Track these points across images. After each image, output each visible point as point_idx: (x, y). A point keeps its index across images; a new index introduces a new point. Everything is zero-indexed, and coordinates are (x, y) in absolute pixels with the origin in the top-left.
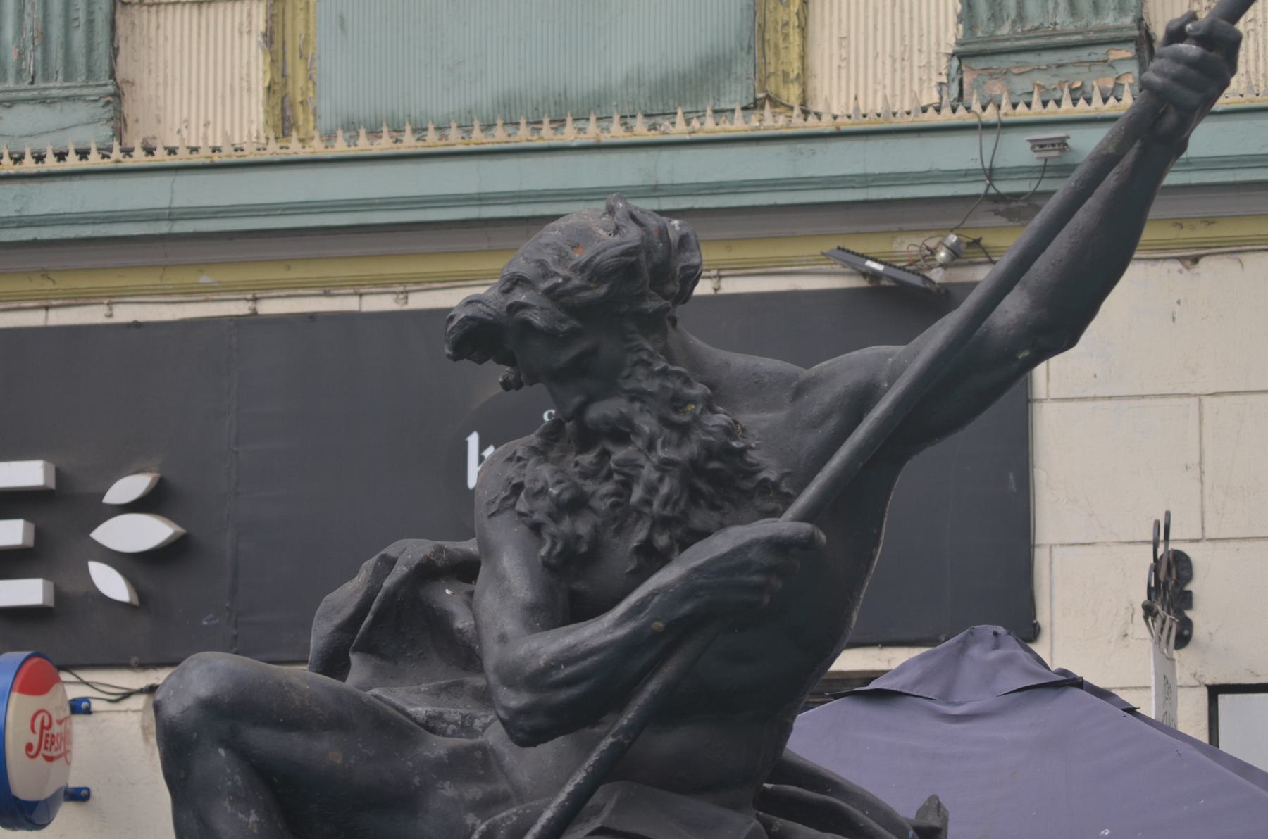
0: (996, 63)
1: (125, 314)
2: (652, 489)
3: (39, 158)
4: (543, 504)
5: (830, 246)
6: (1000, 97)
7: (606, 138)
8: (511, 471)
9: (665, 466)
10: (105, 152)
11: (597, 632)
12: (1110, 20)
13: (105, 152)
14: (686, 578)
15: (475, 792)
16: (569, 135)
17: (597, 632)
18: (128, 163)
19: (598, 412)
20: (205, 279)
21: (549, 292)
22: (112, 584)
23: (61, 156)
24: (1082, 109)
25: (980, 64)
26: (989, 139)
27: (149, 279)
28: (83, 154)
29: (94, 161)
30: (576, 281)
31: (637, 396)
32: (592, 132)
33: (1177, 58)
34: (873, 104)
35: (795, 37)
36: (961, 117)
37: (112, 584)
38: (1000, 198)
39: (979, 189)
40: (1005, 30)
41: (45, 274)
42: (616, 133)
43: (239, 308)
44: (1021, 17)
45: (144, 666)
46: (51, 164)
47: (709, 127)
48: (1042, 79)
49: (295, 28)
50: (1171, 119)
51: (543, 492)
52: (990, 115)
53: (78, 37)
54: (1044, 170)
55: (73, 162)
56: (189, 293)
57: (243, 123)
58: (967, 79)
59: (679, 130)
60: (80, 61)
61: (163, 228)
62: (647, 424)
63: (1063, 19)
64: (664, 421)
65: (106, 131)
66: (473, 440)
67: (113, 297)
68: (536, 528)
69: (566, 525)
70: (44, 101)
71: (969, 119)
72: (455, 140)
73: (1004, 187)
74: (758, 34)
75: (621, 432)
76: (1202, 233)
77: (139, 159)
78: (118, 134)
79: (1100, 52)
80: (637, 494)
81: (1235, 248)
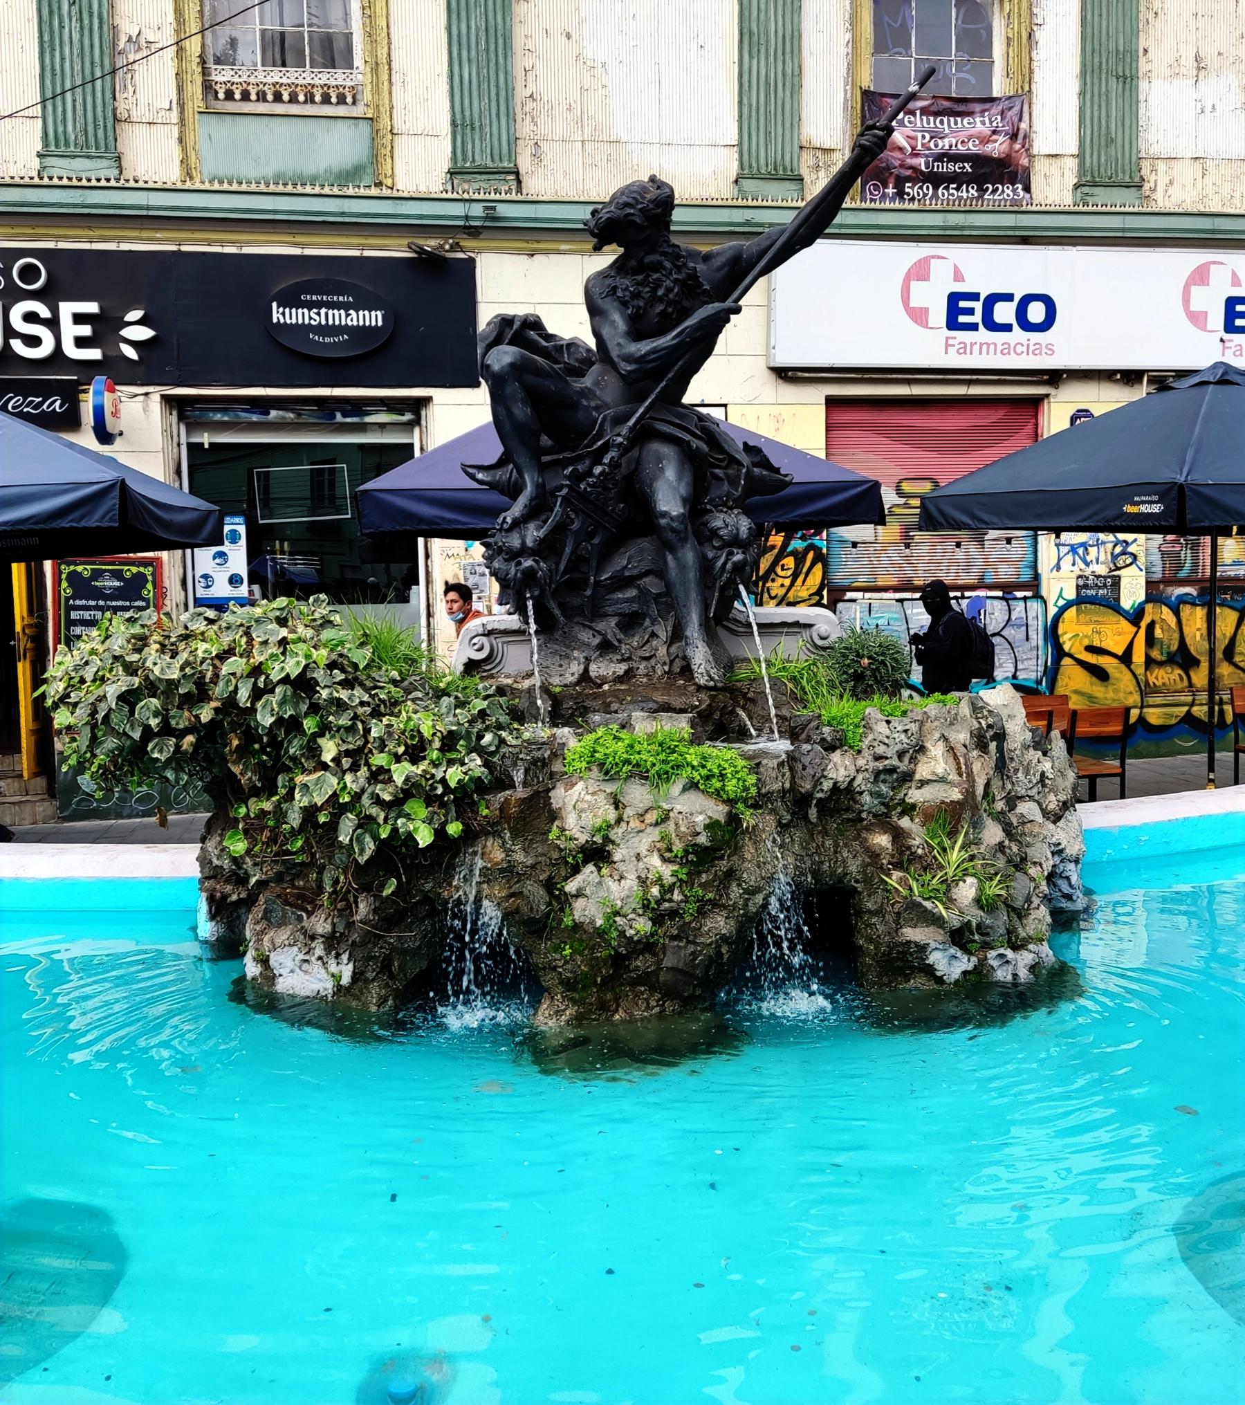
0: (465, 177)
1: (125, 247)
2: (669, 290)
3: (89, 180)
4: (627, 293)
5: (405, 242)
6: (469, 188)
7: (323, 192)
8: (608, 281)
9: (676, 281)
10: (118, 180)
11: (665, 341)
12: (506, 164)
13: (118, 180)
14: (699, 322)
15: (593, 404)
16: (308, 190)
17: (665, 341)
18: (127, 185)
19: (648, 259)
20: (158, 235)
21: (640, 210)
22: (130, 352)
23: (98, 180)
24: (498, 197)
25: (459, 177)
26: (467, 205)
27: (135, 234)
28: (108, 180)
29: (113, 183)
30: (651, 206)
31: (664, 254)
32: (317, 190)
33: (875, 136)
34: (423, 188)
35: (389, 160)
36: (455, 196)
37: (130, 352)
38: (471, 227)
39: (462, 223)
40: (468, 165)
41: (90, 228)
42: (327, 191)
43: (174, 248)
44: (474, 161)
45: (142, 385)
46: (94, 183)
47: (362, 192)
48: (482, 184)
49: (190, 138)
50: (868, 159)
51: (626, 289)
52: (466, 196)
53: (101, 133)
54: (487, 218)
55: (103, 183)
56: (151, 240)
57: (171, 174)
58: (455, 182)
59: (351, 192)
60: (102, 143)
61: (144, 213)
62: (668, 265)
63: (489, 162)
64: (674, 264)
65: (117, 172)
66: (274, 305)
67: (120, 239)
68: (624, 304)
69: (635, 302)
70: (88, 157)
71: (459, 197)
72: (263, 188)
73: (472, 223)
74: (374, 157)
75: (657, 267)
76: (536, 246)
77: (132, 184)
78: (121, 173)
79: (503, 176)
80: (660, 292)
81: (546, 252)
